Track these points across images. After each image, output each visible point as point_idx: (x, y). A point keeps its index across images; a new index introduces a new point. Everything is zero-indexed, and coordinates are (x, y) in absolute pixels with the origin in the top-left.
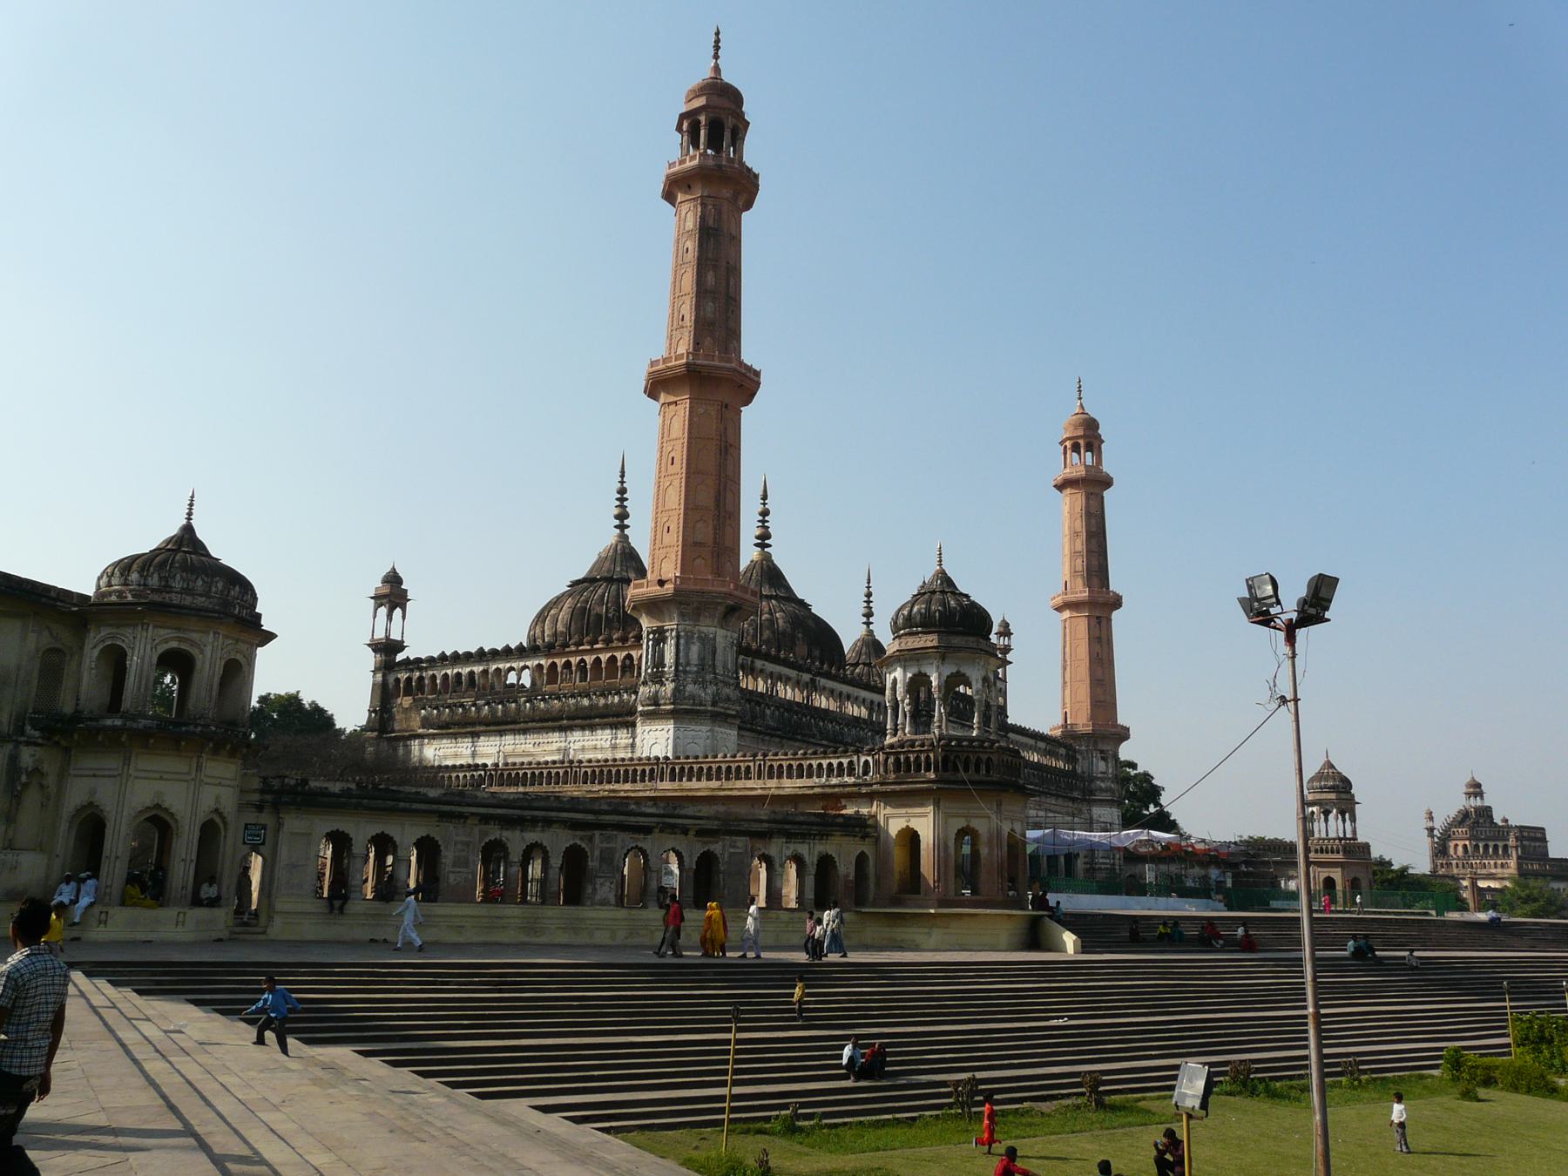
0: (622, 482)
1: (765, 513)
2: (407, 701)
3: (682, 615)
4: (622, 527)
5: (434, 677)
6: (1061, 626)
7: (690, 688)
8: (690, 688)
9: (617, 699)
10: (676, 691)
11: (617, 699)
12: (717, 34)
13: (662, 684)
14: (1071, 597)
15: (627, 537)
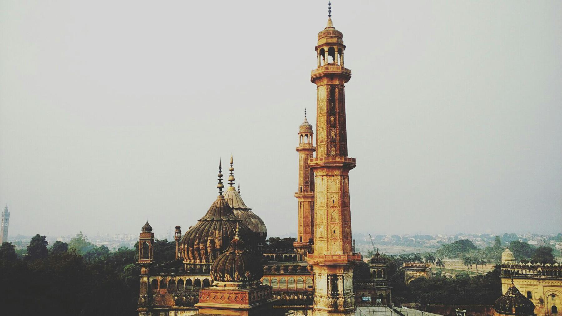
0: (220, 172)
1: (232, 170)
2: (163, 291)
3: (344, 270)
4: (221, 193)
5: (181, 281)
6: (297, 205)
7: (349, 300)
8: (349, 300)
9: (296, 297)
10: (345, 302)
11: (296, 297)
12: (330, 4)
13: (338, 299)
14: (306, 194)
15: (223, 197)
